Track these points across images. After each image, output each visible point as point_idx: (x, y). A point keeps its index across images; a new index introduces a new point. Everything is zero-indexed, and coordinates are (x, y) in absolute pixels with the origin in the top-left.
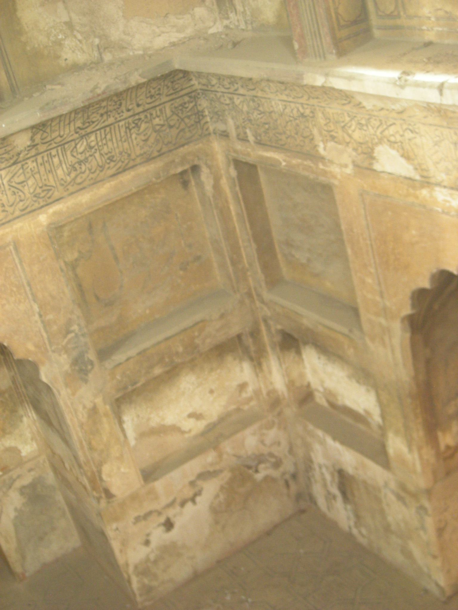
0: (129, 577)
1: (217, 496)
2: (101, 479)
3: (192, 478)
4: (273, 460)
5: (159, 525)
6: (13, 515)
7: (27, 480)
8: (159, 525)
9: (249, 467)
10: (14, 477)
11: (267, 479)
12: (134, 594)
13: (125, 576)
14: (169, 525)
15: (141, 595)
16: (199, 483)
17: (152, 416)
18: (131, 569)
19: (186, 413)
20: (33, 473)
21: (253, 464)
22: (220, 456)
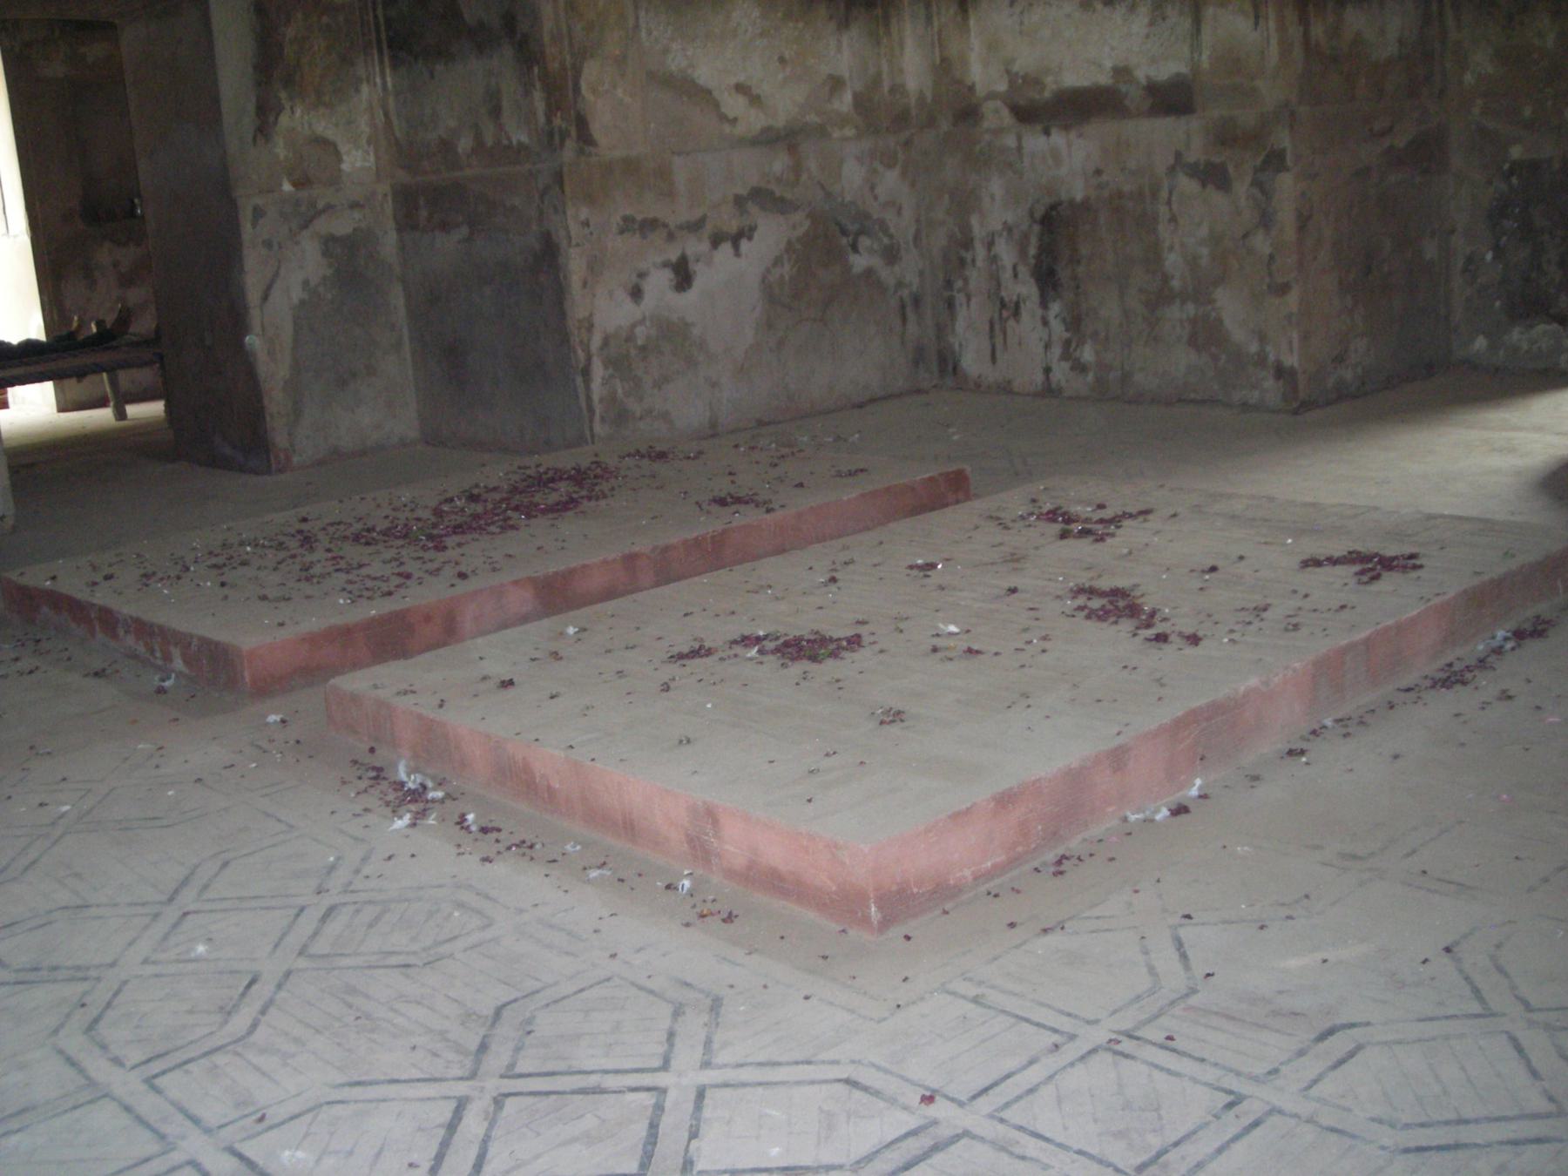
0: (589, 359)
1: (777, 262)
2: (577, 90)
3: (743, 192)
4: (886, 241)
5: (666, 265)
6: (297, 294)
7: (342, 225)
8: (666, 265)
9: (844, 232)
10: (321, 204)
11: (869, 272)
12: (591, 410)
13: (581, 354)
14: (683, 276)
15: (603, 419)
16: (752, 208)
17: (675, 46)
18: (596, 341)
19: (733, 80)
20: (357, 215)
21: (853, 227)
22: (797, 169)
